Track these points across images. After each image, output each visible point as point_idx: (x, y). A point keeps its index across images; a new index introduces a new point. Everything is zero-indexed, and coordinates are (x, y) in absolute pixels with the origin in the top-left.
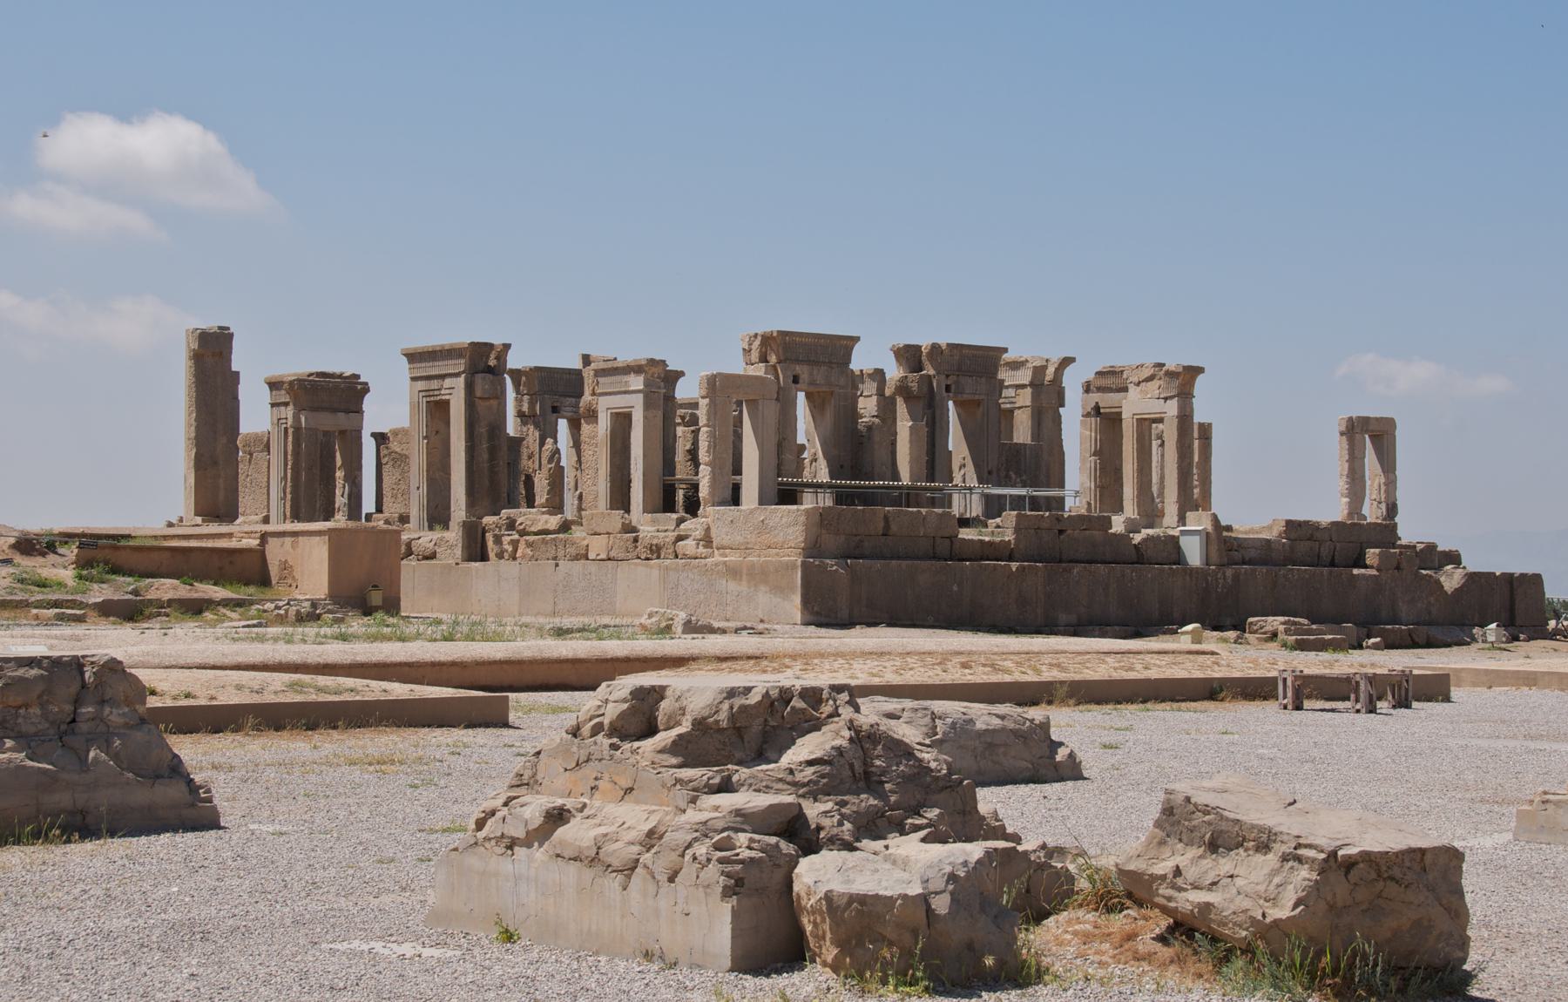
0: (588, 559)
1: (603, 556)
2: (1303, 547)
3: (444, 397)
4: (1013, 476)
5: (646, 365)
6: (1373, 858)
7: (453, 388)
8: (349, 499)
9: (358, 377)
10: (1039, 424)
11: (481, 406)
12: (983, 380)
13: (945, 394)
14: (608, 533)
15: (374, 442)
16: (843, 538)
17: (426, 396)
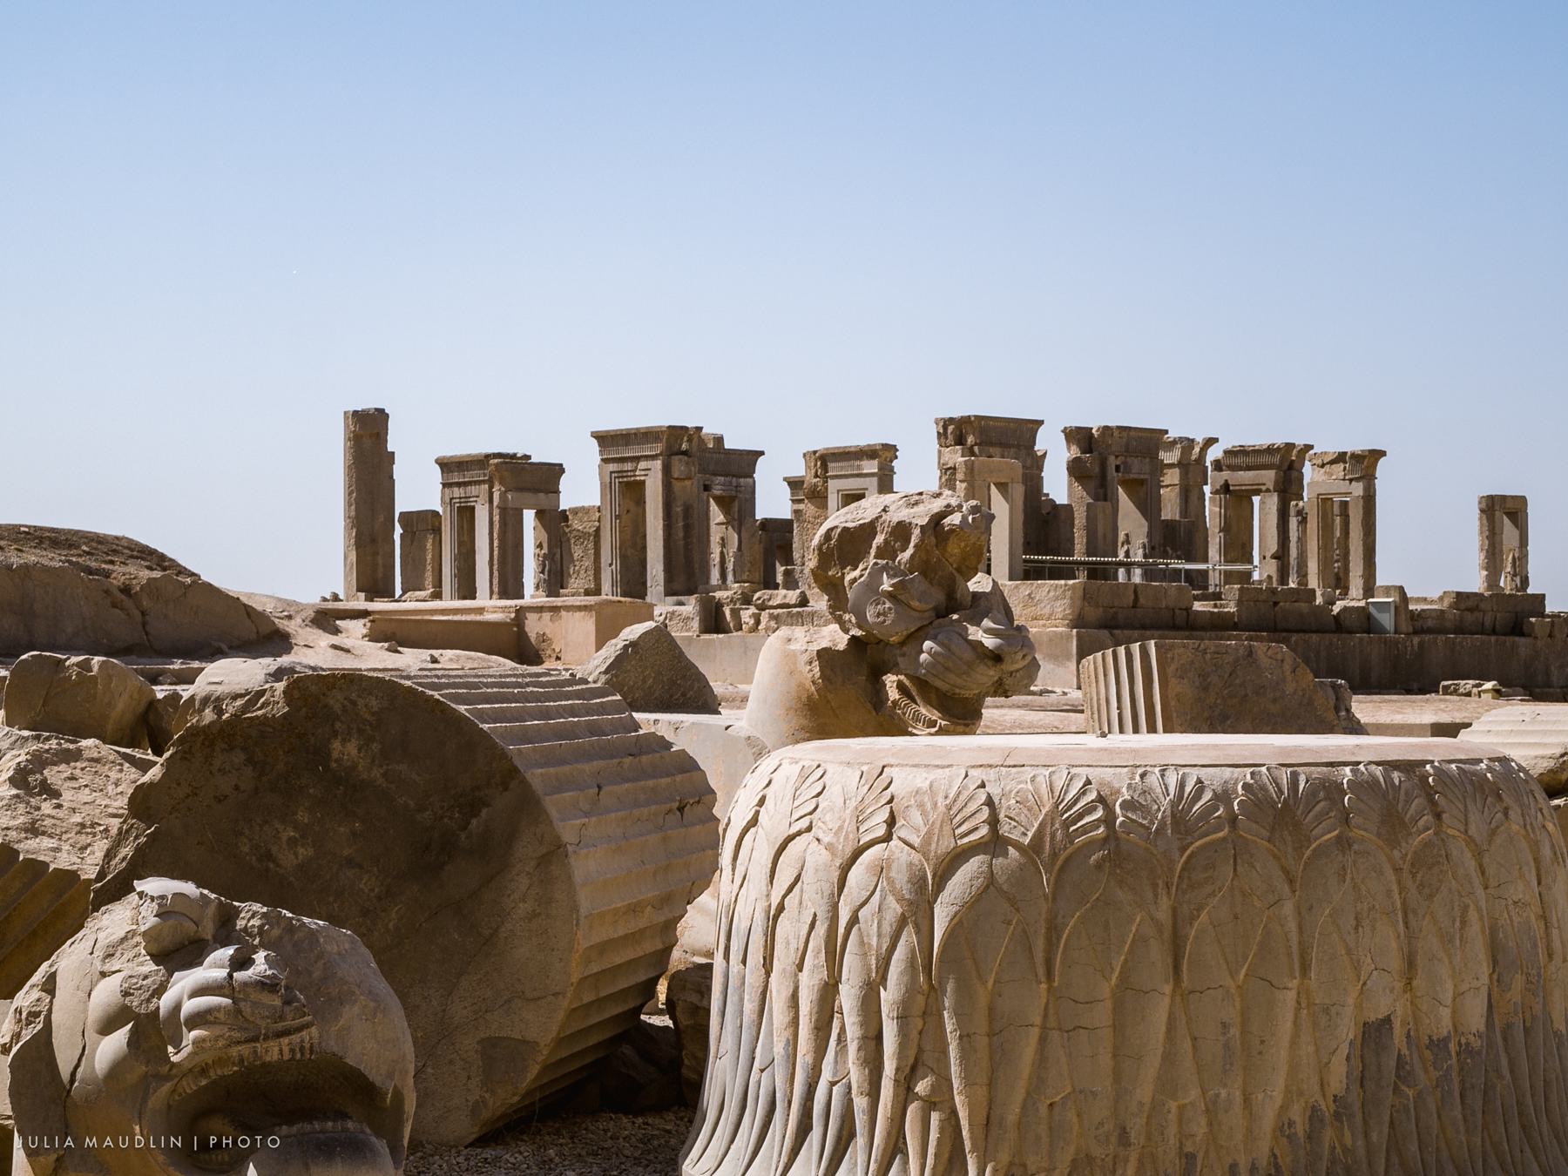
2: (1469, 617)
3: (638, 478)
4: (1170, 552)
5: (880, 450)
7: (649, 469)
8: (549, 576)
9: (529, 457)
10: (1186, 502)
11: (677, 486)
12: (1147, 460)
13: (1115, 474)
15: (992, 525)
16: (1101, 609)
17: (619, 477)
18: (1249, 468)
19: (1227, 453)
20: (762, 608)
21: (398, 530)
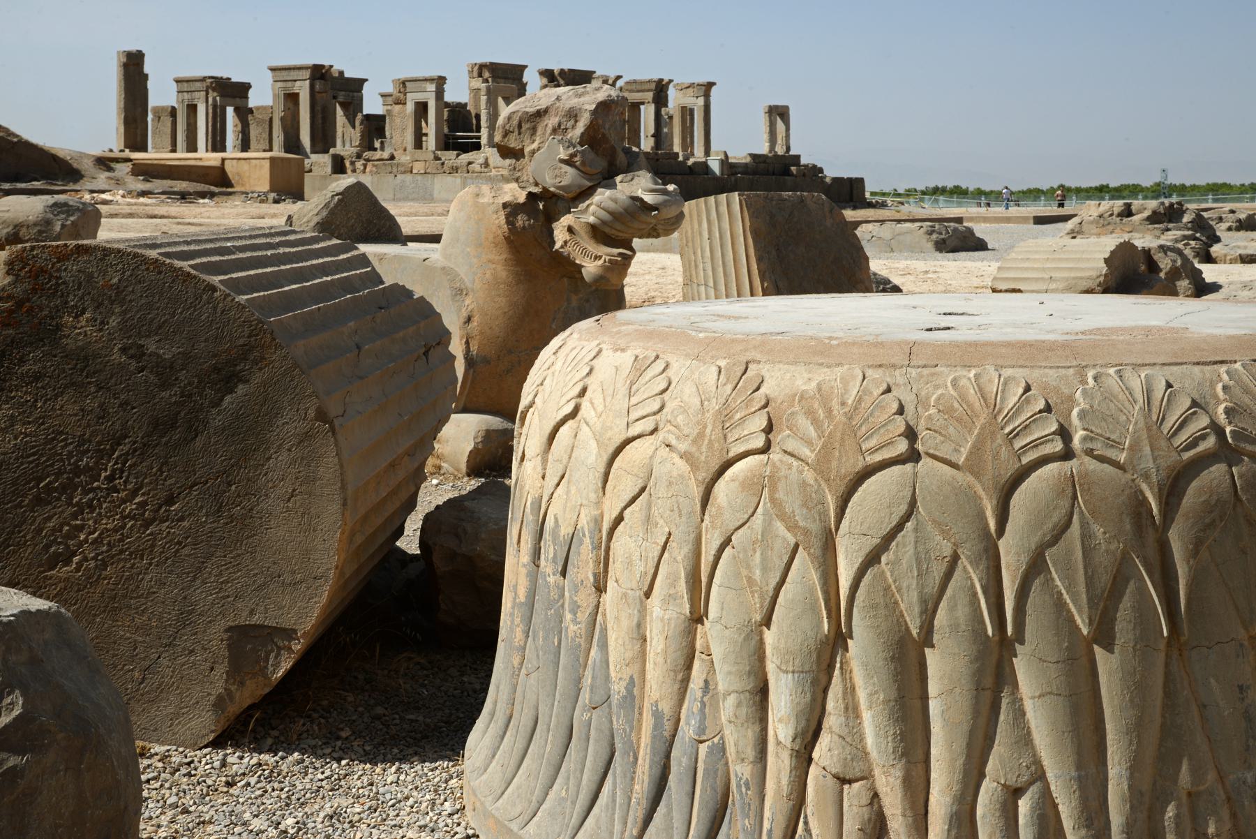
9: (230, 79)
18: (638, 91)
19: (627, 83)
20: (368, 160)
21: (150, 117)
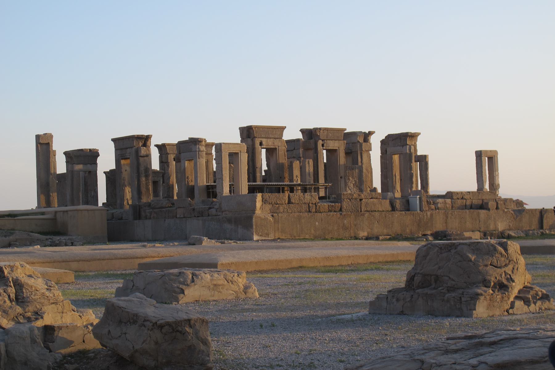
0: (177, 218)
1: (182, 216)
6: (169, 323)
14: (184, 207)
